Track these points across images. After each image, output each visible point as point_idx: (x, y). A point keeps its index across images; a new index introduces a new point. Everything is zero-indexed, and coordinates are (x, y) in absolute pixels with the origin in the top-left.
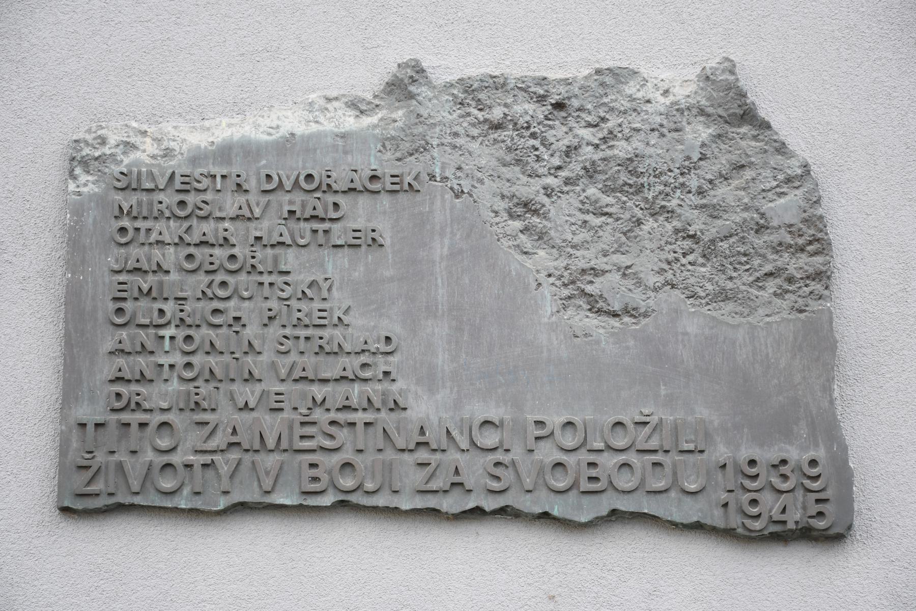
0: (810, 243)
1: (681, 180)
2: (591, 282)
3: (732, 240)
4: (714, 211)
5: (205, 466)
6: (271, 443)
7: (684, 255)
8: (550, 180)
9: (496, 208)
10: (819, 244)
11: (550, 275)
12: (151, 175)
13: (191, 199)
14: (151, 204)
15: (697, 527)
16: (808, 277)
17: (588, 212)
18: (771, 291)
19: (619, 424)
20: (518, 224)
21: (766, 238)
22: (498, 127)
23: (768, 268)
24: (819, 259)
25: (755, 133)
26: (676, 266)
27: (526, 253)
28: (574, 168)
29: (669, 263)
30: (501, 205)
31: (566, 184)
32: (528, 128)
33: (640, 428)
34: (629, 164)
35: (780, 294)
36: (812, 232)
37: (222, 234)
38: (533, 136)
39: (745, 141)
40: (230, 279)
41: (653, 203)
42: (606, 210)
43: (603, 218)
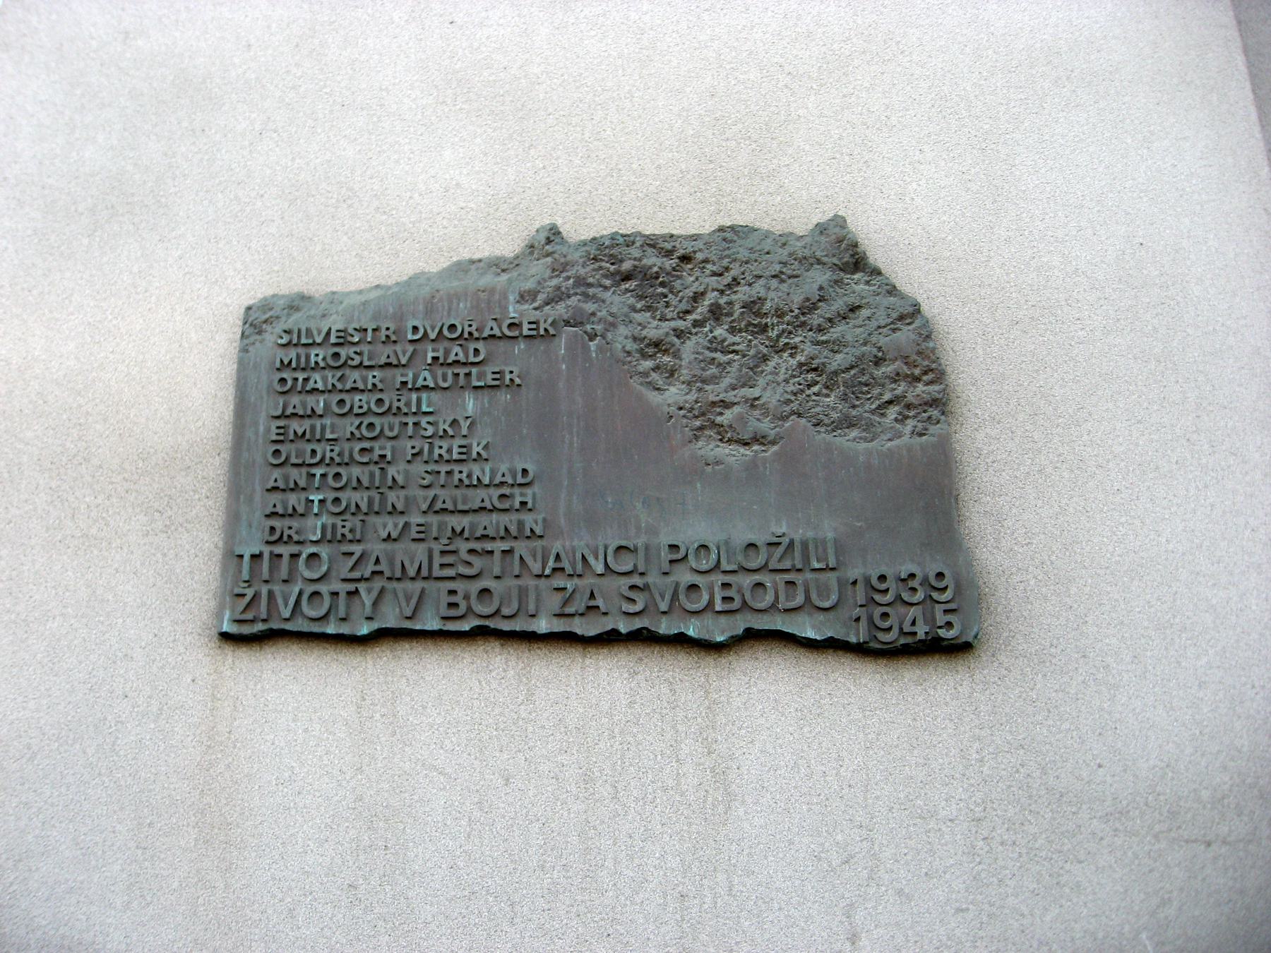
0: (925, 373)
1: (802, 319)
2: (721, 414)
3: (853, 372)
4: (837, 346)
5: (349, 593)
6: (412, 572)
7: (809, 386)
8: (680, 324)
9: (628, 348)
10: (937, 374)
11: (681, 409)
12: (308, 331)
13: (343, 352)
14: (308, 357)
15: (832, 645)
16: (926, 404)
17: (716, 350)
18: (893, 417)
19: (752, 545)
20: (649, 364)
21: (884, 369)
22: (627, 277)
23: (887, 397)
24: (936, 387)
25: (867, 278)
26: (800, 397)
27: (658, 389)
28: (702, 310)
29: (795, 394)
30: (631, 346)
31: (694, 326)
32: (657, 278)
33: (773, 548)
34: (752, 306)
35: (902, 419)
36: (926, 363)
37: (370, 381)
38: (663, 284)
39: (858, 285)
40: (377, 421)
41: (777, 341)
42: (736, 348)
43: (730, 356)
